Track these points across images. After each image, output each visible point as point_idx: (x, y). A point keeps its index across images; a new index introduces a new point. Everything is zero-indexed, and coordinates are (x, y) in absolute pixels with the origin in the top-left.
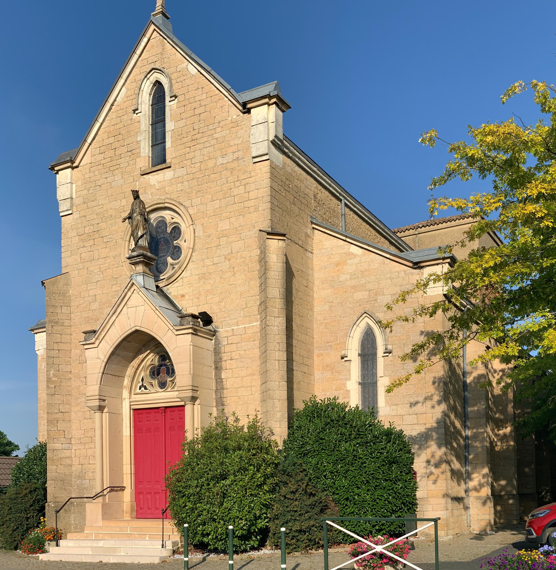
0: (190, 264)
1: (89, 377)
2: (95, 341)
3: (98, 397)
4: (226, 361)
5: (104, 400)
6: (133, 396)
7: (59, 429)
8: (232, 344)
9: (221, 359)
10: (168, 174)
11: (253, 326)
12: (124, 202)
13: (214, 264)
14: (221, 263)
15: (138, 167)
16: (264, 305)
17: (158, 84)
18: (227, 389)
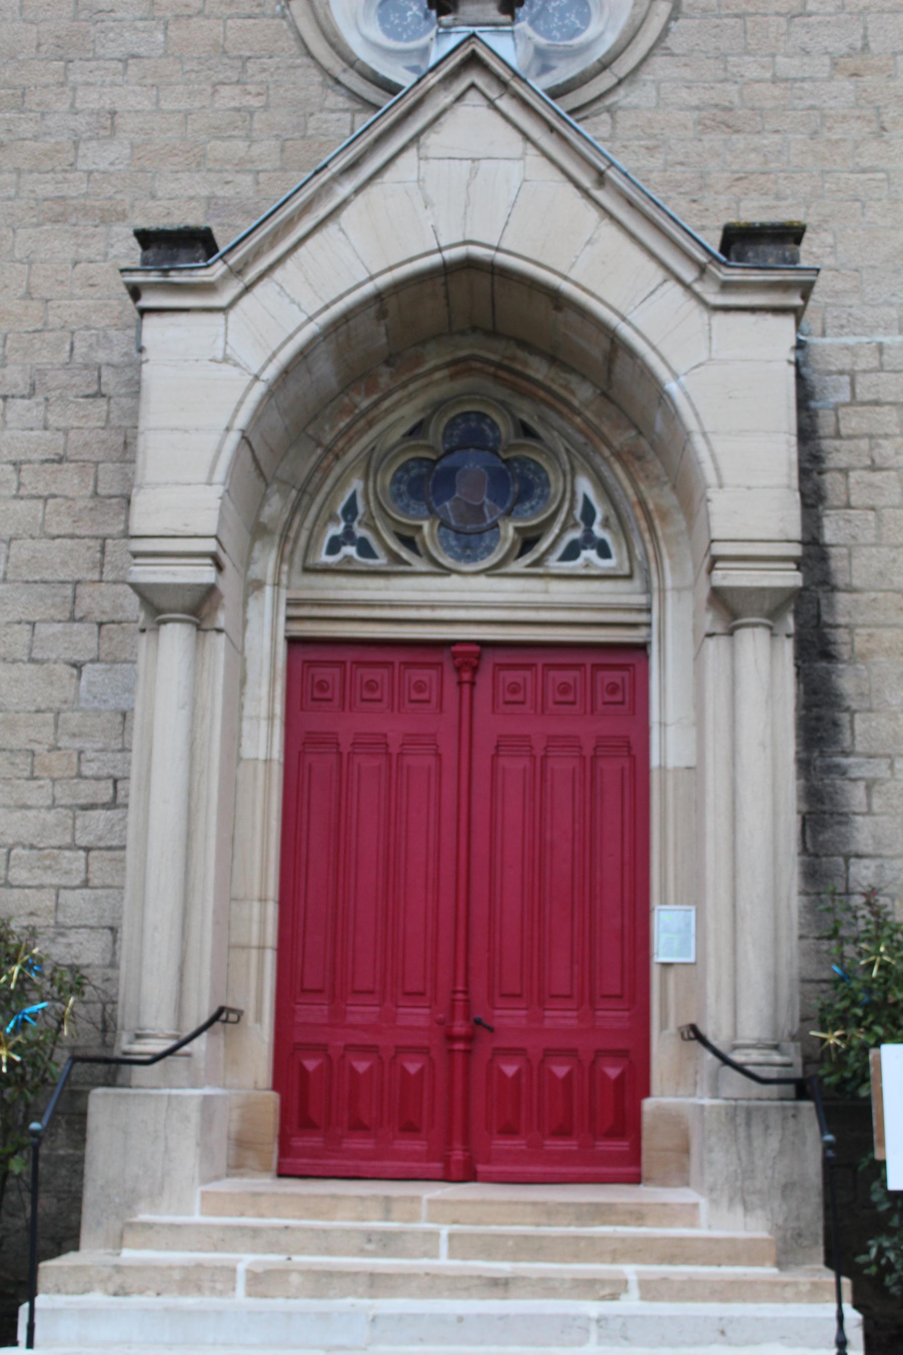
0: (658, 61)
4: (845, 471)
8: (877, 403)
14: (813, 79)
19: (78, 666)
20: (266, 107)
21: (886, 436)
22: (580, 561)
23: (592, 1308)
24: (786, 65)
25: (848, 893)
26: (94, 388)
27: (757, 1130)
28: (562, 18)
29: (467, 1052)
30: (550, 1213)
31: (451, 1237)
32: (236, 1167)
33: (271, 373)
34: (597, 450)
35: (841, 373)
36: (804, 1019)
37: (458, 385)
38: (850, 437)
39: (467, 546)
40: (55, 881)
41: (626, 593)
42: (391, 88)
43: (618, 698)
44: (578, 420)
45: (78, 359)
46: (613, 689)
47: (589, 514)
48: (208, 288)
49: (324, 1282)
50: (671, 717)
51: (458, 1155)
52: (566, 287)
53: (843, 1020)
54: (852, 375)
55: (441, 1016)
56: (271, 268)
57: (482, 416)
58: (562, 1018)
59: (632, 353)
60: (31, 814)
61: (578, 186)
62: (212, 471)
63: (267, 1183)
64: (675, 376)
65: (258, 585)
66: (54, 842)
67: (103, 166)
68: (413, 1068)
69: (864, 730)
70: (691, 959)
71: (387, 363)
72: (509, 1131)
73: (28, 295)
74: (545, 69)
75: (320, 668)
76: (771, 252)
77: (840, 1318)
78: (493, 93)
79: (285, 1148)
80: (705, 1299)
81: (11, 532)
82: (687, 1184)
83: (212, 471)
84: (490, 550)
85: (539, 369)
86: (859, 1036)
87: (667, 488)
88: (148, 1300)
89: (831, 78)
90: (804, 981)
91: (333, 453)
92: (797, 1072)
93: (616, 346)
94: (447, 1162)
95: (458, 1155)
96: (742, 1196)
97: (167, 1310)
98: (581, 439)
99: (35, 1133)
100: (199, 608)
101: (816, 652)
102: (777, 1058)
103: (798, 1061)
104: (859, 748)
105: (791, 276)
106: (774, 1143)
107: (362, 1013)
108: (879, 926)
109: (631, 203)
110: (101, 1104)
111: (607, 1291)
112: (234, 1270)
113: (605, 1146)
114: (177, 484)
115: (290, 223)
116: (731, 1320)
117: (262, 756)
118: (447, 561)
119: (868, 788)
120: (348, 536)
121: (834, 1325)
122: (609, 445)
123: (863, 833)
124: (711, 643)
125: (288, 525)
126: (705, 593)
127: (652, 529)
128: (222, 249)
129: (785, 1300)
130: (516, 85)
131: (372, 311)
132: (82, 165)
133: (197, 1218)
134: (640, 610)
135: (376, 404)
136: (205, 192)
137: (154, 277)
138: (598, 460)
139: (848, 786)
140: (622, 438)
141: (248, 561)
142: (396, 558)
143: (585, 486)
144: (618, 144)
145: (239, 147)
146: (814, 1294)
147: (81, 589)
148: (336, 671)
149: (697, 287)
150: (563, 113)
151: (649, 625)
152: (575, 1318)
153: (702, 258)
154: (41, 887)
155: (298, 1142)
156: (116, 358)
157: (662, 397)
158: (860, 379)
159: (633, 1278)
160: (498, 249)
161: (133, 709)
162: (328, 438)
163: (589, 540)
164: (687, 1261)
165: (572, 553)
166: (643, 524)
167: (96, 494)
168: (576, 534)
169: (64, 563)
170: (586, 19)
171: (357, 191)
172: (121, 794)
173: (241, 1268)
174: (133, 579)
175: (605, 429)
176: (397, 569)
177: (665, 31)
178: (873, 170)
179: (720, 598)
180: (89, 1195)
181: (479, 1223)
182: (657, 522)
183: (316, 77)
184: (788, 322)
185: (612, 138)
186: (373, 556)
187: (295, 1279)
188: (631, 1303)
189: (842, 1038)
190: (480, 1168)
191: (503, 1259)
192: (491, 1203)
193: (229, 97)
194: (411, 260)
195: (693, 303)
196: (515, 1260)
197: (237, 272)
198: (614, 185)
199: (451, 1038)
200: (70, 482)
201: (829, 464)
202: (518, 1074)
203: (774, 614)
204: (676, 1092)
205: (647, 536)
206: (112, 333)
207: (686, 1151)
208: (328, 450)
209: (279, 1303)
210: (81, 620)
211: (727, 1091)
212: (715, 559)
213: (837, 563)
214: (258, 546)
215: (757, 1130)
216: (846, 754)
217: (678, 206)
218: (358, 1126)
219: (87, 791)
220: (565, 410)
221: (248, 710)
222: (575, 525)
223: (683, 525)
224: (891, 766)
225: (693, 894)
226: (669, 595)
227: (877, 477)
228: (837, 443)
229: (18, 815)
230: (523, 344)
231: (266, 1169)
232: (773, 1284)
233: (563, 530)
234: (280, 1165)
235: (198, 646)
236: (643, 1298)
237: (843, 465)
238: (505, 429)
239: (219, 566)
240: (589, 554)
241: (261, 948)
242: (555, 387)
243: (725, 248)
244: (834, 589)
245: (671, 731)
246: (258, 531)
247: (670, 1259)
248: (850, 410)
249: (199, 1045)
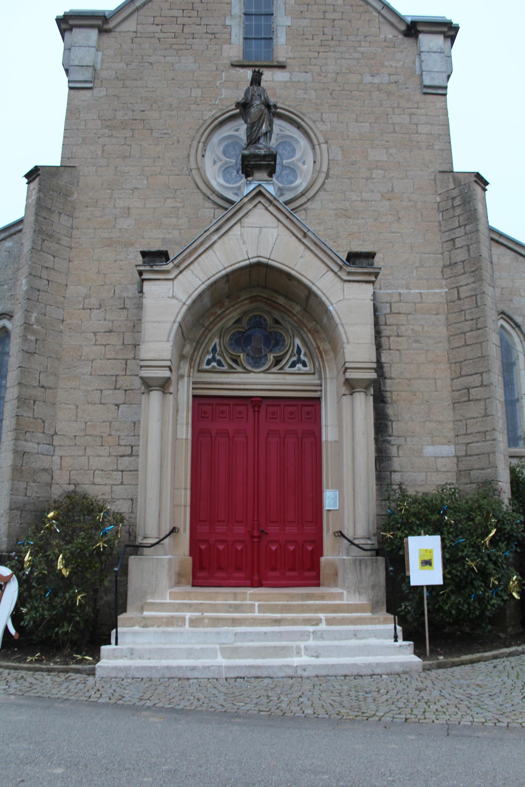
0: (321, 193)
4: (389, 337)
7: (36, 416)
8: (399, 313)
11: (436, 293)
14: (375, 201)
15: (225, 55)
19: (118, 405)
20: (183, 207)
21: (402, 325)
22: (296, 368)
23: (311, 628)
24: (366, 196)
25: (391, 484)
26: (122, 306)
27: (363, 567)
28: (287, 177)
29: (259, 542)
30: (292, 597)
31: (259, 606)
32: (178, 583)
33: (189, 302)
34: (302, 329)
35: (387, 303)
36: (377, 528)
37: (253, 305)
38: (390, 325)
39: (256, 363)
40: (111, 482)
41: (313, 380)
42: (231, 202)
43: (310, 416)
44: (295, 318)
45: (116, 295)
46: (308, 413)
47: (299, 351)
48: (167, 272)
49: (216, 622)
50: (329, 423)
51: (256, 578)
52: (293, 273)
53: (392, 528)
55: (249, 529)
56: (189, 265)
57: (261, 317)
58: (291, 530)
59: (316, 296)
60: (102, 458)
61: (297, 237)
62: (169, 337)
63: (189, 588)
64: (332, 304)
65: (182, 377)
66: (111, 468)
67: (125, 227)
68: (239, 548)
69: (396, 428)
70: (338, 508)
71: (228, 297)
72: (274, 569)
73: (99, 272)
74: (282, 195)
75: (205, 407)
76: (365, 262)
77: (395, 628)
78: (267, 204)
79: (194, 577)
80: (348, 624)
81: (93, 357)
82: (337, 586)
83: (169, 337)
84: (264, 364)
85: (281, 300)
86: (399, 534)
87: (327, 343)
88: (155, 629)
89: (381, 201)
90: (377, 515)
91: (208, 329)
92: (376, 547)
93: (310, 293)
94: (252, 580)
95: (256, 578)
96: (358, 590)
97: (163, 632)
98: (296, 325)
99: (116, 572)
100: (164, 385)
101: (380, 400)
102: (369, 542)
103: (376, 543)
104: (394, 434)
105: (371, 270)
106: (369, 571)
107: (221, 528)
108: (404, 496)
109: (316, 244)
110: (133, 561)
111: (315, 623)
112: (185, 618)
113: (307, 574)
114: (156, 341)
115: (196, 249)
116: (358, 631)
117: (184, 437)
118: (249, 368)
119: (398, 448)
120: (214, 359)
121: (393, 631)
122: (306, 327)
123: (396, 463)
124: (345, 398)
125: (193, 355)
126: (342, 380)
127: (322, 357)
128: (171, 258)
129: (375, 624)
130: (275, 202)
131: (224, 280)
132: (117, 226)
133: (168, 601)
134: (318, 386)
135: (224, 312)
136: (161, 236)
137: (148, 268)
138: (302, 332)
139: (391, 447)
140: (311, 325)
141: (179, 368)
142: (231, 367)
143: (298, 341)
144: (308, 221)
145: (174, 221)
146: (385, 622)
147: (118, 378)
148: (210, 407)
149: (339, 273)
150: (289, 210)
151: (321, 391)
152: (305, 632)
153: (341, 263)
154: (106, 485)
155: (199, 574)
156: (130, 295)
157: (327, 311)
158: (393, 305)
159: (323, 618)
160: (269, 259)
161: (139, 421)
162: (206, 324)
163: (299, 361)
164: (341, 612)
165: (293, 365)
166: (319, 355)
167: (123, 344)
168: (295, 358)
169: (112, 369)
170: (296, 178)
171: (219, 238)
172: (134, 451)
173: (187, 617)
174: (141, 375)
175: (305, 321)
176: (231, 371)
177: (324, 183)
178: (396, 232)
179: (348, 382)
180: (130, 593)
181: (267, 601)
182: (323, 355)
183: (201, 196)
184: (370, 287)
185: (306, 219)
186: (223, 366)
187: (206, 621)
188: (323, 626)
189: (392, 535)
190: (264, 582)
191: (277, 613)
192: (272, 594)
193: (170, 203)
194: (238, 262)
195: (337, 279)
196: (282, 613)
197: (177, 266)
198: (310, 238)
199: (253, 537)
200: (114, 340)
201: (383, 334)
202: (276, 549)
203: (367, 388)
204: (332, 554)
205: (320, 359)
206: (129, 286)
207: (337, 575)
208: (207, 328)
209: (201, 629)
210: (119, 389)
211: (353, 554)
212: (346, 369)
213: (386, 369)
214: (182, 362)
215: (363, 567)
216: (390, 436)
217: (330, 244)
218: (220, 568)
219: (122, 450)
220: (291, 315)
221: (179, 421)
222: (295, 355)
223: (333, 356)
224: (406, 440)
225: (339, 486)
226: (328, 380)
227: (399, 339)
228: (386, 327)
229: (97, 459)
230: (276, 291)
231: (188, 584)
232: (371, 619)
233: (290, 357)
234: (193, 582)
235: (164, 398)
236: (327, 624)
237: (388, 335)
238: (269, 321)
239: (171, 370)
240: (299, 366)
241: (185, 506)
242: (287, 307)
243: (348, 259)
244: (385, 378)
245: (329, 428)
246: (182, 357)
247: (335, 612)
248: (390, 315)
249: (167, 540)
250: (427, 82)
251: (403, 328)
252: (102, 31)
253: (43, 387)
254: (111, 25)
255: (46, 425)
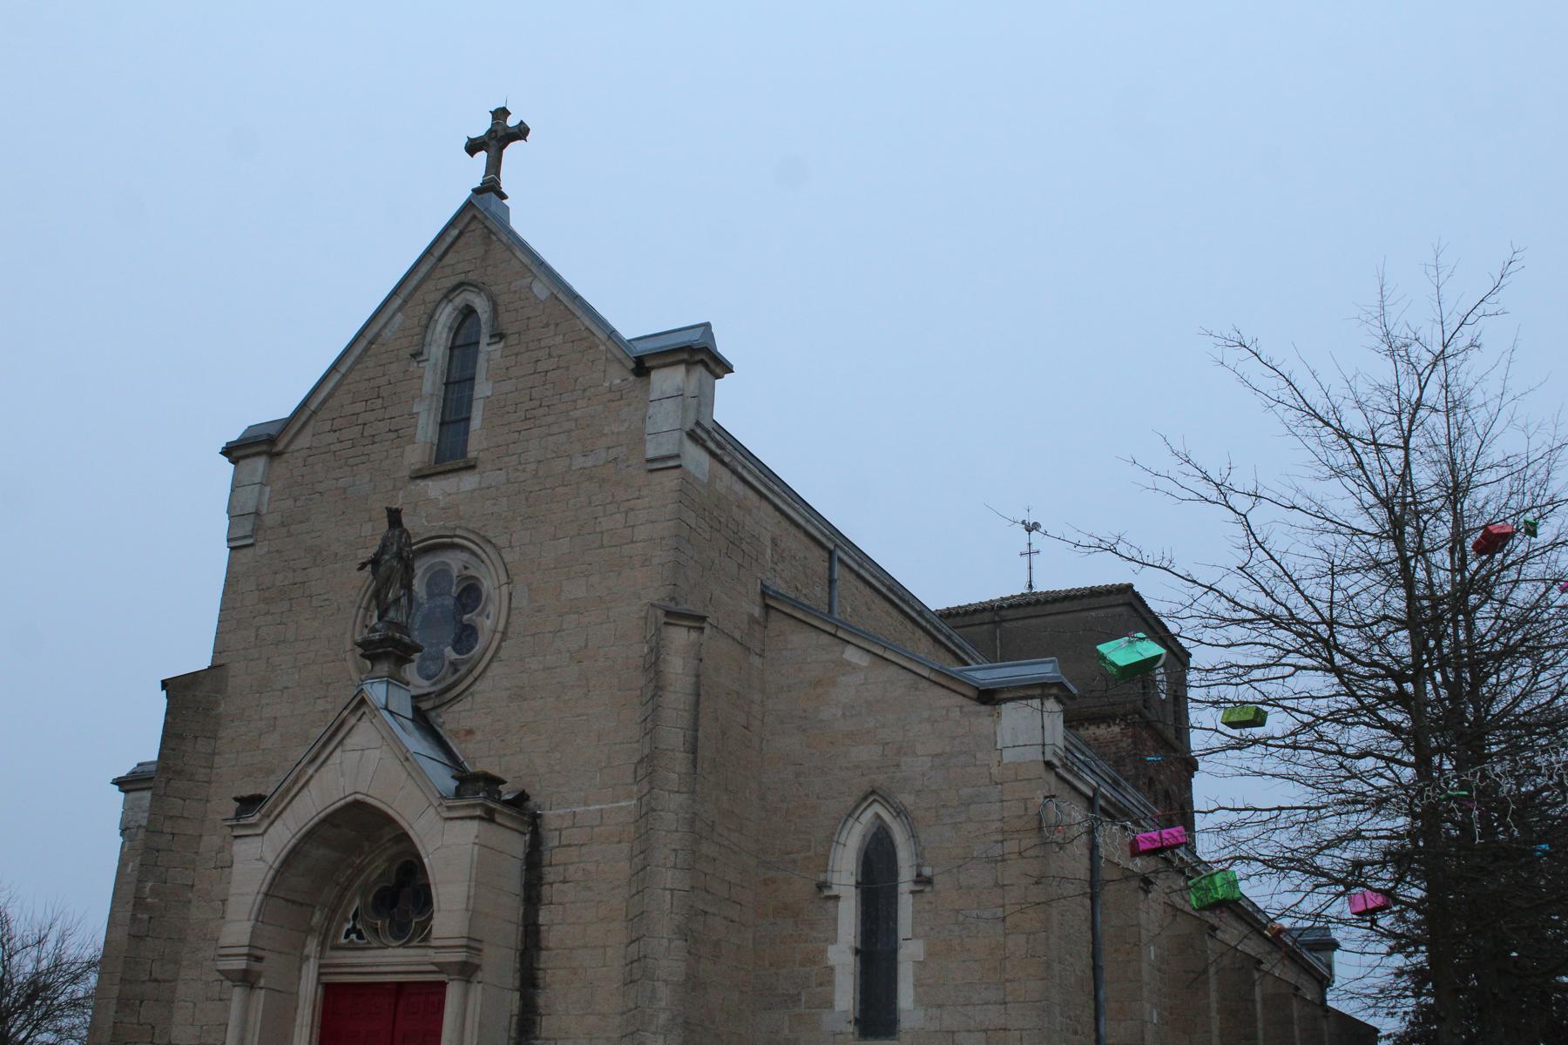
0: (495, 665)
1: (231, 900)
2: (261, 819)
3: (245, 950)
4: (551, 884)
5: (259, 959)
6: (328, 953)
9: (540, 878)
10: (468, 481)
11: (621, 808)
12: (367, 529)
13: (544, 670)
16: (648, 765)
17: (468, 312)
18: (548, 949)
33: (276, 865)
54: (560, 830)
115: (289, 790)
120: (353, 930)
177: (498, 648)
213: (543, 935)
244: (540, 949)
250: (650, 454)
251: (572, 868)
252: (273, 456)
253: (156, 980)
254: (280, 446)
255: (157, 1032)
